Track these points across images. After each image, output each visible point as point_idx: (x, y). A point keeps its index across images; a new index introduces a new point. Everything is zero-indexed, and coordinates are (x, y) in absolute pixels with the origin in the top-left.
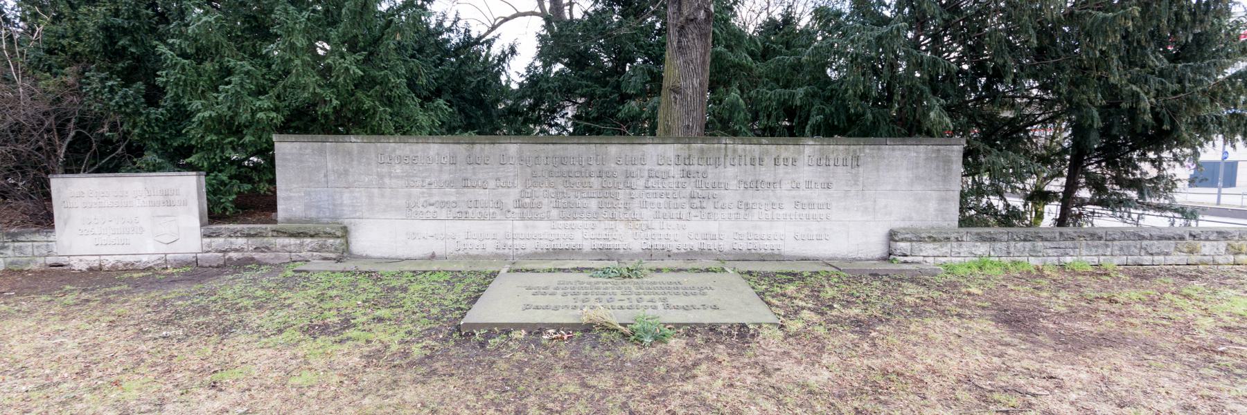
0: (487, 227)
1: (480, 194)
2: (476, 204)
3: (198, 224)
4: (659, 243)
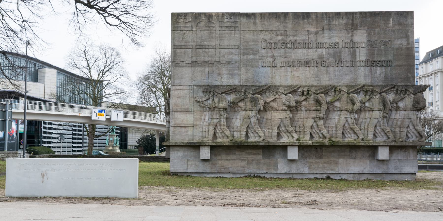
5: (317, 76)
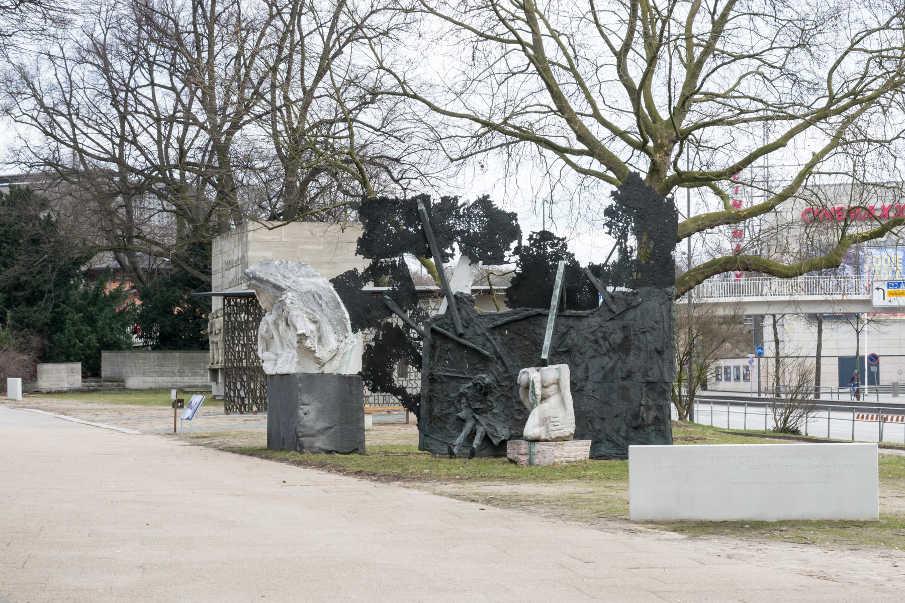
0: (169, 379)
1: (167, 369)
2: (165, 372)
3: (80, 378)
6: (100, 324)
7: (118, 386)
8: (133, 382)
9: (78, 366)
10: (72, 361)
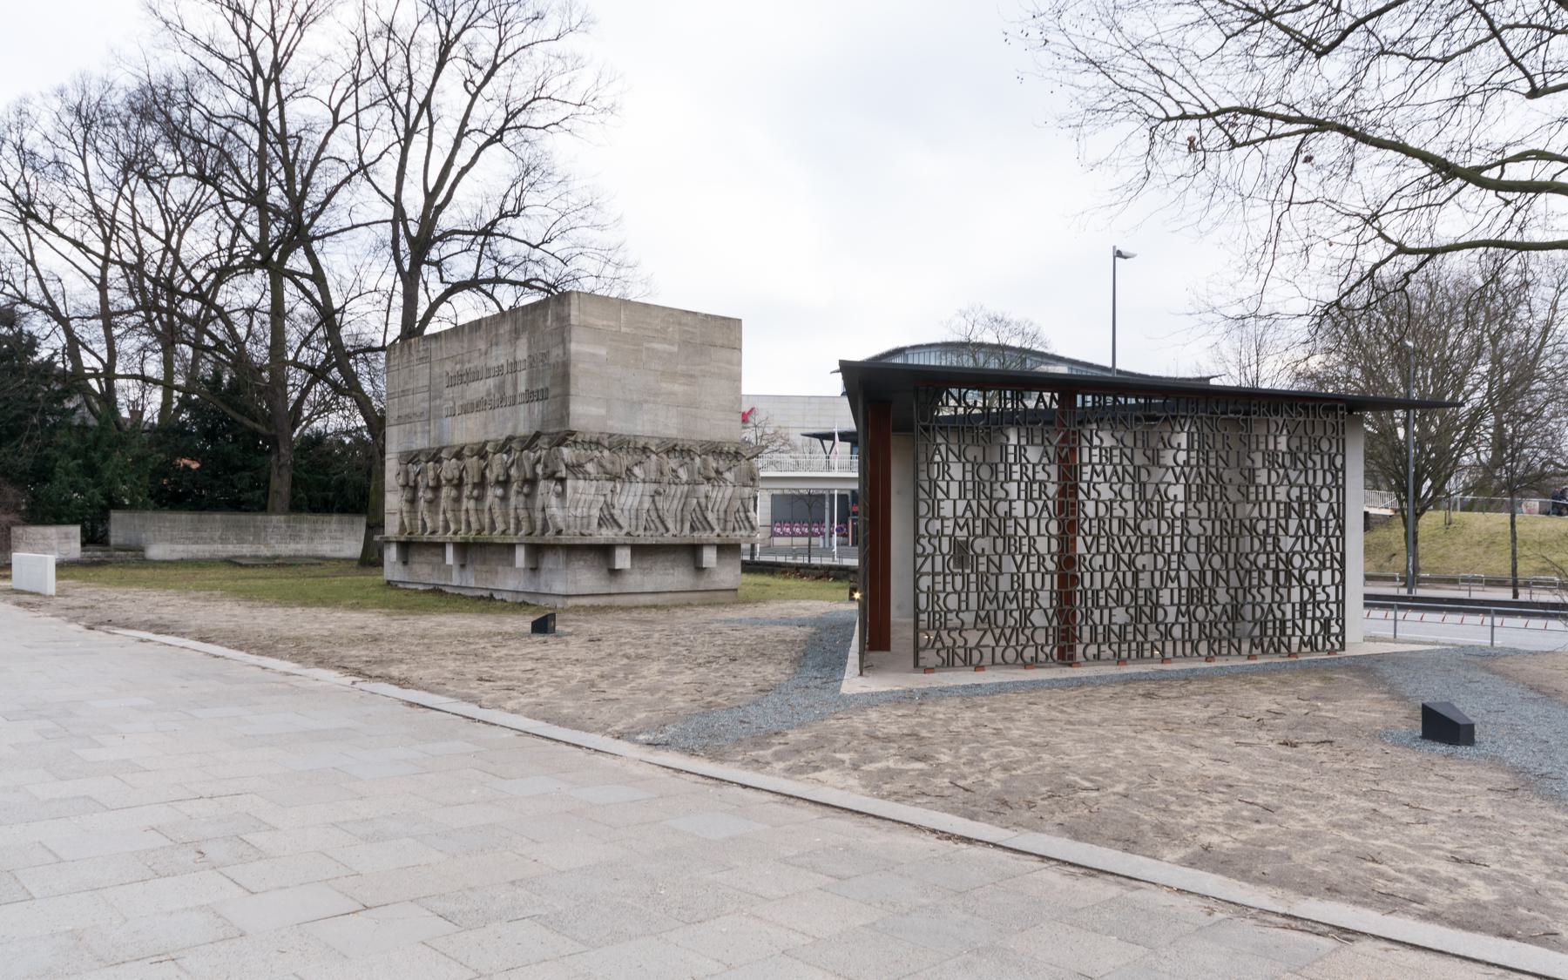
0: (206, 547)
1: (204, 534)
3: (78, 545)
4: (277, 553)
5: (485, 426)
6: (107, 474)
7: (135, 557)
8: (156, 551)
9: (76, 530)
10: (63, 523)
